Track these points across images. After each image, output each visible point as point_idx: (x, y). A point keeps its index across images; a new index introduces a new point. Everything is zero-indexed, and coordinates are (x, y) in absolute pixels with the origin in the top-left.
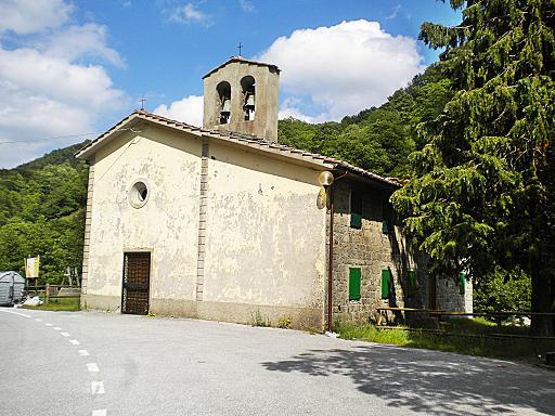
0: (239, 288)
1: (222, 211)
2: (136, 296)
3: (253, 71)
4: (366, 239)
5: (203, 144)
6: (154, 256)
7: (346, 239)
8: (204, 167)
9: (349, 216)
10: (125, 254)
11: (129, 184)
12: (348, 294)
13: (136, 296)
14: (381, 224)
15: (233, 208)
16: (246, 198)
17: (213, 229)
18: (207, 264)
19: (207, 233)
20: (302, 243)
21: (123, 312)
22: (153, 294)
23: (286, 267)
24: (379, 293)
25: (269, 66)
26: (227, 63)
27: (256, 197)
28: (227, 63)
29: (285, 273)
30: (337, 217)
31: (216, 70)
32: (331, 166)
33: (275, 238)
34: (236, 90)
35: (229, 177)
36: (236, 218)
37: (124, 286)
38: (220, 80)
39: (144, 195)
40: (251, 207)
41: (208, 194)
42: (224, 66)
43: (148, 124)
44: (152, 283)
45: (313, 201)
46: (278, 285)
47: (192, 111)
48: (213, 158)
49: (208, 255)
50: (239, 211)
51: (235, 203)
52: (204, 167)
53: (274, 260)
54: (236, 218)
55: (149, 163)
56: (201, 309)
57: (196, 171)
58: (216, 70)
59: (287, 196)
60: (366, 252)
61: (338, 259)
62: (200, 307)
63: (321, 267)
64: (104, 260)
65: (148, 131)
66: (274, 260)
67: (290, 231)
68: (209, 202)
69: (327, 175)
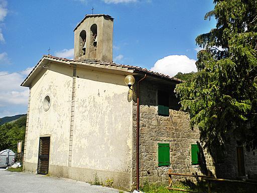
0: (88, 158)
1: (81, 109)
2: (43, 166)
3: (96, 21)
4: (175, 123)
5: (73, 69)
6: (51, 139)
7: (154, 123)
8: (74, 83)
9: (157, 107)
10: (41, 138)
11: (44, 97)
12: (157, 162)
13: (43, 166)
14: (157, 107)
15: (86, 107)
16: (92, 100)
17: (77, 121)
18: (74, 142)
19: (74, 123)
20: (120, 127)
21: (38, 173)
22: (51, 163)
23: (111, 143)
24: (189, 160)
25: (104, 16)
26: (84, 19)
27: (98, 99)
28: (84, 19)
29: (111, 147)
30: (144, 108)
31: (80, 25)
32: (132, 71)
33: (106, 124)
34: (89, 34)
35: (87, 87)
36: (87, 112)
37: (39, 157)
38: (81, 30)
39: (49, 101)
40: (94, 105)
41: (76, 99)
42: (83, 21)
43: (52, 62)
44: (50, 156)
45: (126, 97)
46: (107, 157)
47: (70, 54)
48: (78, 77)
49: (74, 137)
50: (88, 108)
51: (87, 103)
52: (74, 83)
53: (105, 139)
54: (87, 112)
55: (51, 84)
56: (71, 173)
57: (70, 86)
58: (80, 25)
59: (112, 95)
60: (175, 131)
61: (145, 137)
62: (70, 171)
63: (130, 143)
64: (32, 142)
65: (52, 66)
66: (105, 139)
67: (113, 119)
68: (76, 105)
69: (130, 78)
